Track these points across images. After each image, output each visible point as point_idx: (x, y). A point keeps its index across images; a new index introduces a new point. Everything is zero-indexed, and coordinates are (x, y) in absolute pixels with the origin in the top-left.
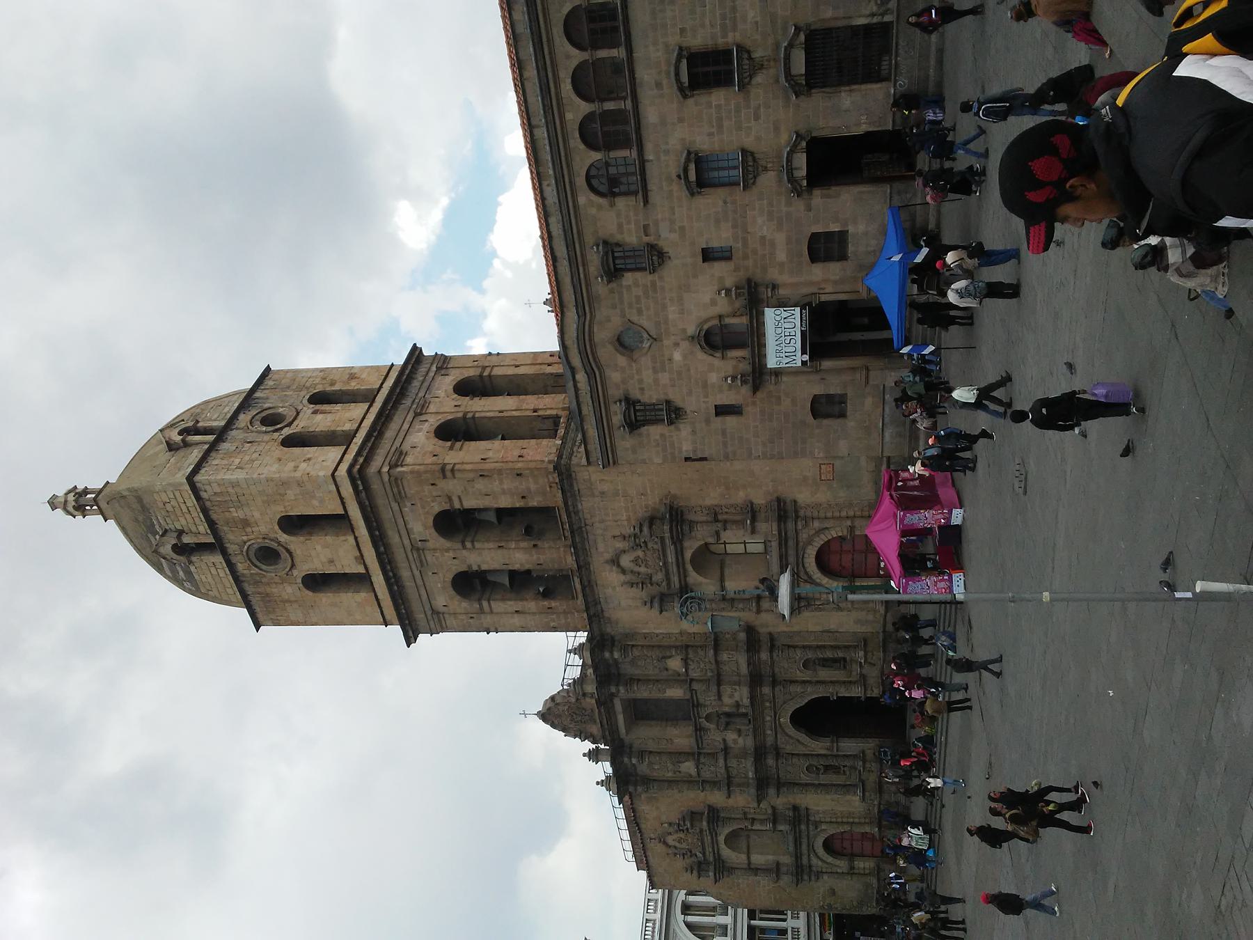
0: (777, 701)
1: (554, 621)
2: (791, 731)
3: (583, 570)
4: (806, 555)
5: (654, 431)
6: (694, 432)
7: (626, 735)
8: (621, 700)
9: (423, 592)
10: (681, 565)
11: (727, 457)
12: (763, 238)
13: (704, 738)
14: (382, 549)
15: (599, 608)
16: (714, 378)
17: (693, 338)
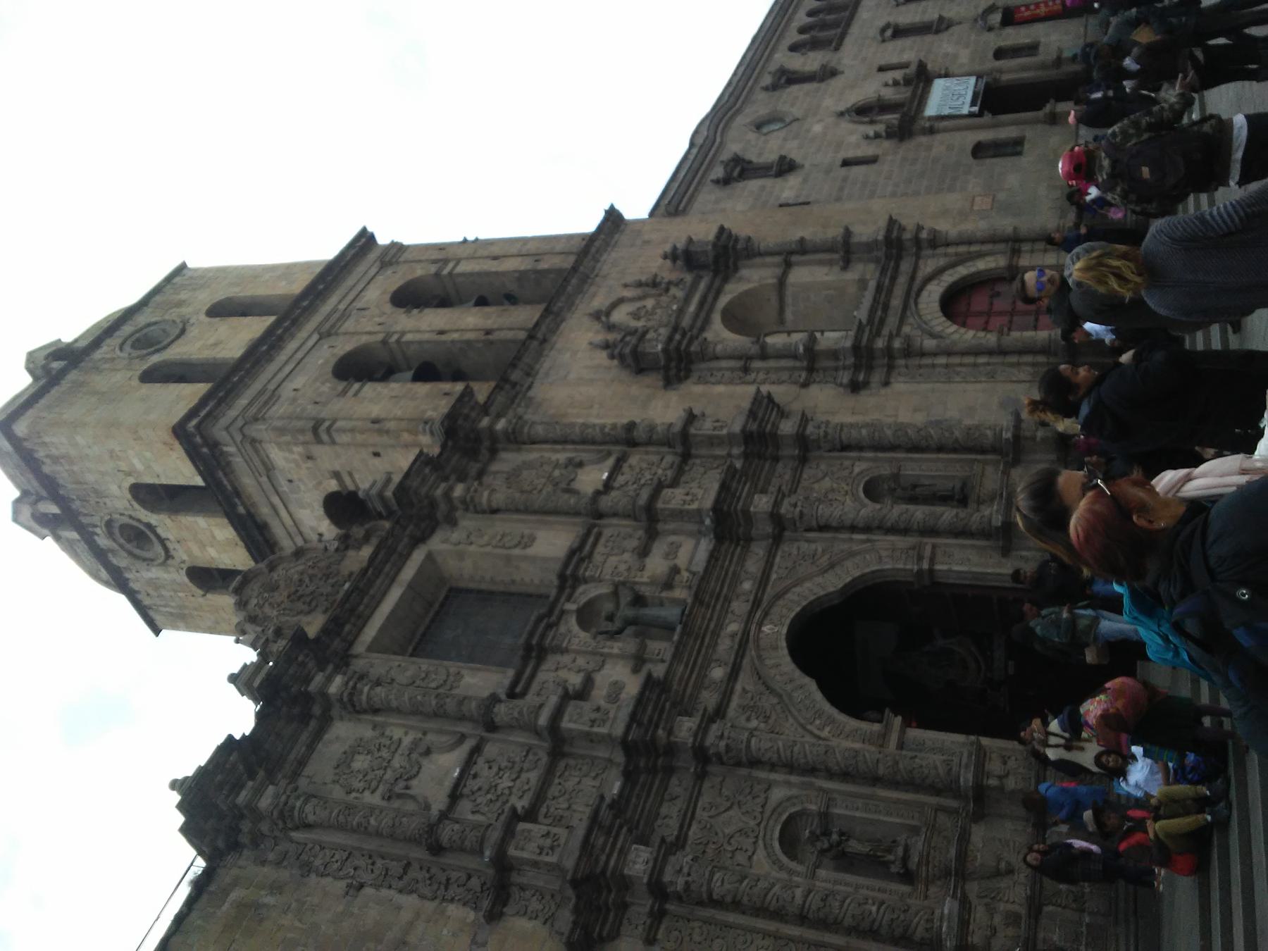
0: (774, 576)
1: (435, 409)
2: (782, 664)
3: (551, 317)
4: (925, 294)
5: (754, 185)
6: (805, 181)
7: (371, 649)
8: (430, 557)
9: (287, 369)
10: (706, 307)
11: (838, 199)
12: (947, 55)
13: (544, 667)
14: (305, 303)
15: (526, 386)
16: (853, 139)
17: (841, 114)
